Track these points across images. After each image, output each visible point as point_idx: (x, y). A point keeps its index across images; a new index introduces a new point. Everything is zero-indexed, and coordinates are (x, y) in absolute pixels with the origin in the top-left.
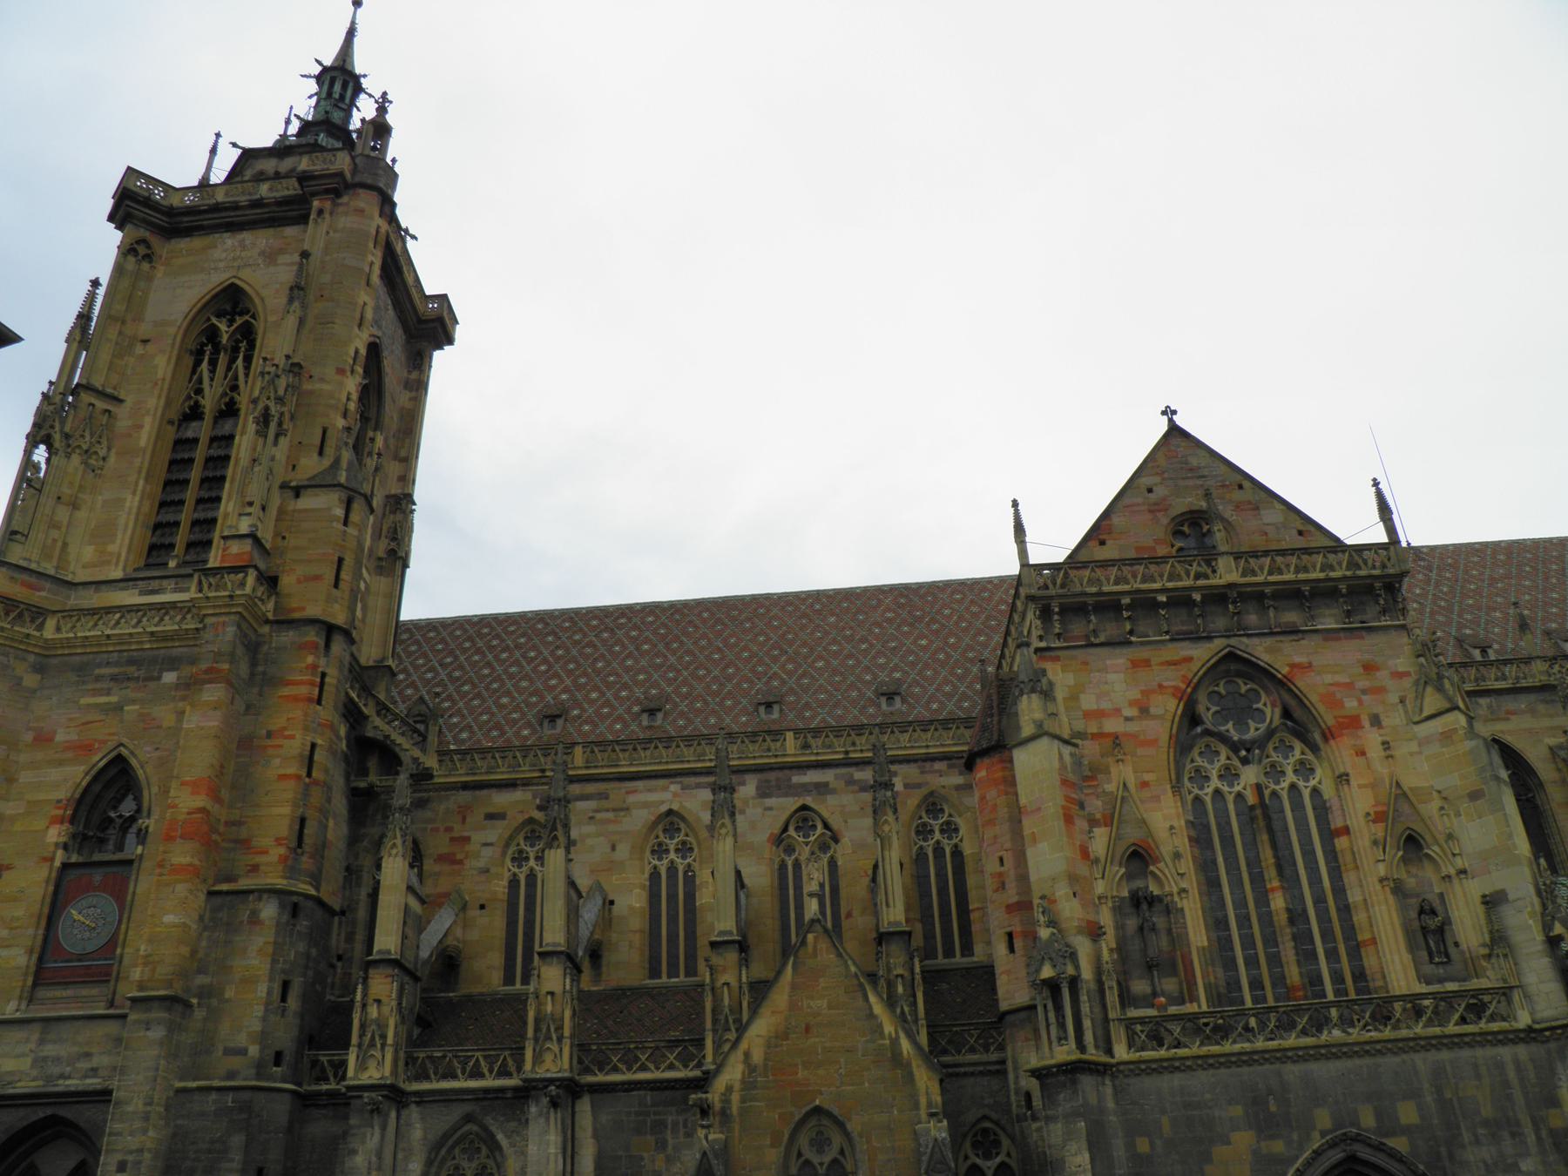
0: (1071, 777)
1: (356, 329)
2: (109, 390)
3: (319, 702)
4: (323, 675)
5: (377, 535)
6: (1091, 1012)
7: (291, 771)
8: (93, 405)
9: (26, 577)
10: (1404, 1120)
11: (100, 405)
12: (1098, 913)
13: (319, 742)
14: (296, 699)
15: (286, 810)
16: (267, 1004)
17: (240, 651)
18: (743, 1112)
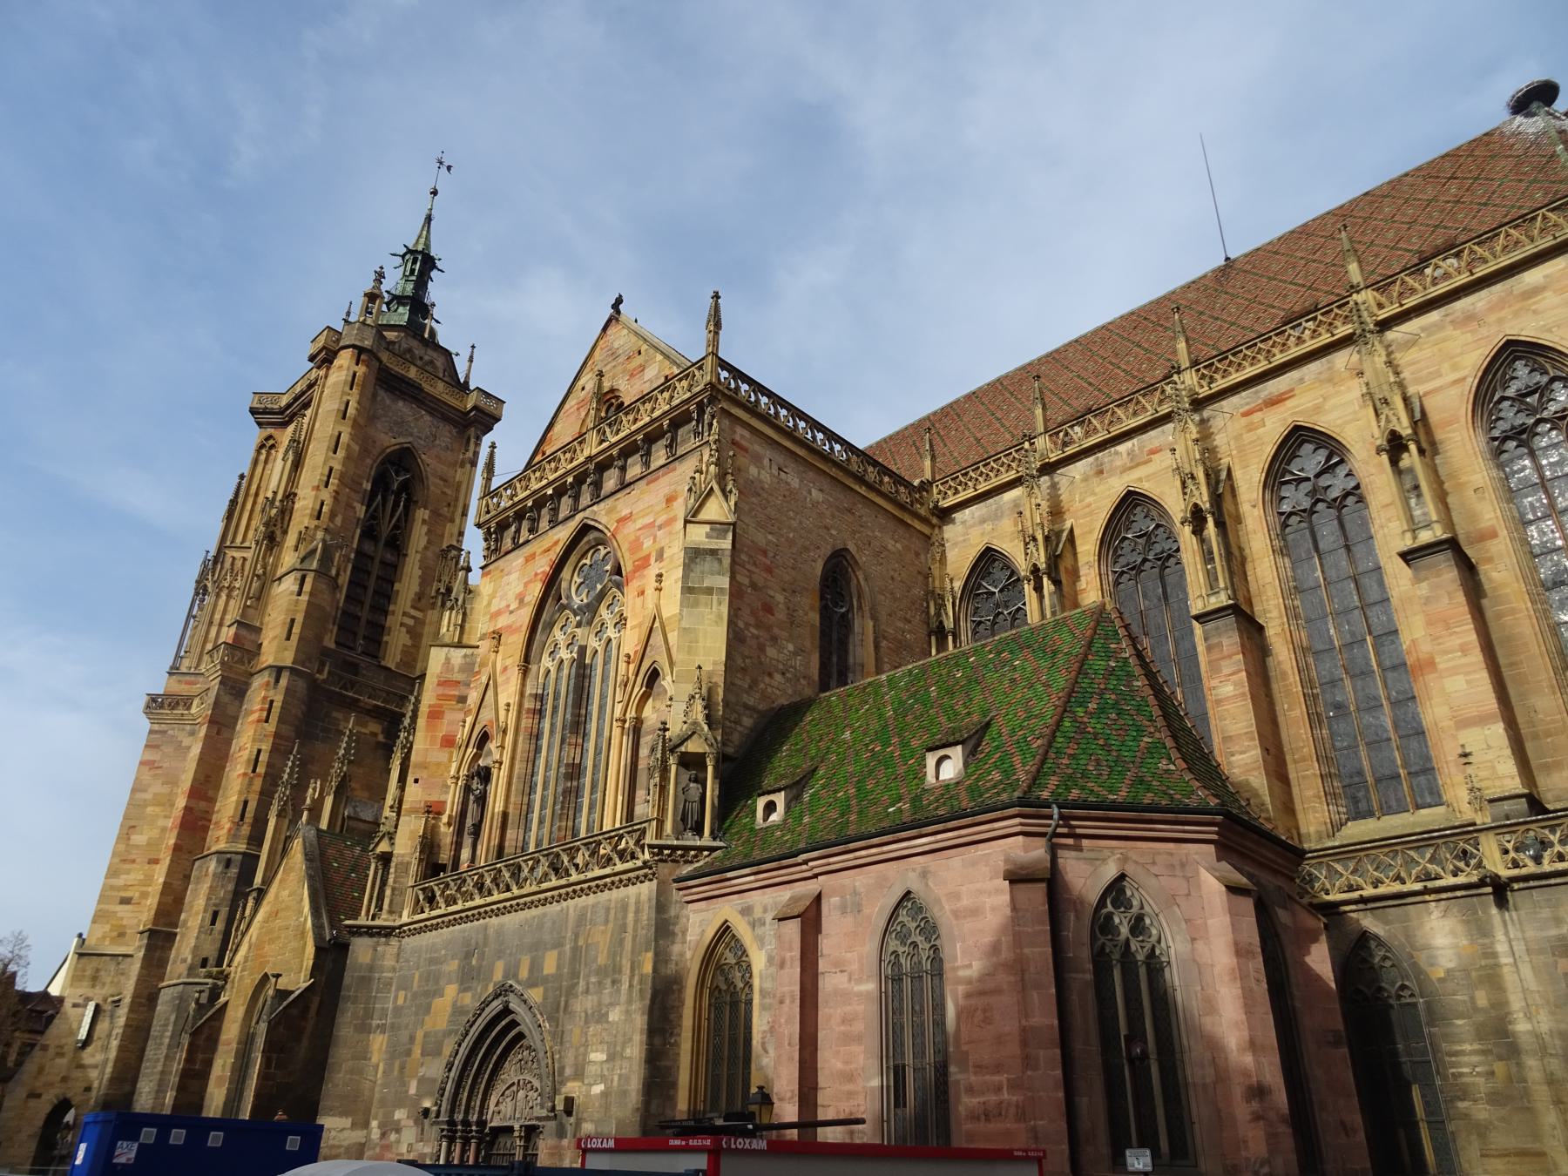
0: (457, 677)
1: (331, 454)
2: (245, 545)
3: (267, 721)
4: (272, 702)
5: (425, 581)
6: (395, 882)
7: (242, 771)
8: (234, 558)
9: (187, 678)
10: (546, 972)
11: (237, 554)
12: (447, 793)
13: (264, 747)
14: (253, 722)
15: (234, 798)
16: (201, 927)
17: (226, 698)
18: (241, 978)
